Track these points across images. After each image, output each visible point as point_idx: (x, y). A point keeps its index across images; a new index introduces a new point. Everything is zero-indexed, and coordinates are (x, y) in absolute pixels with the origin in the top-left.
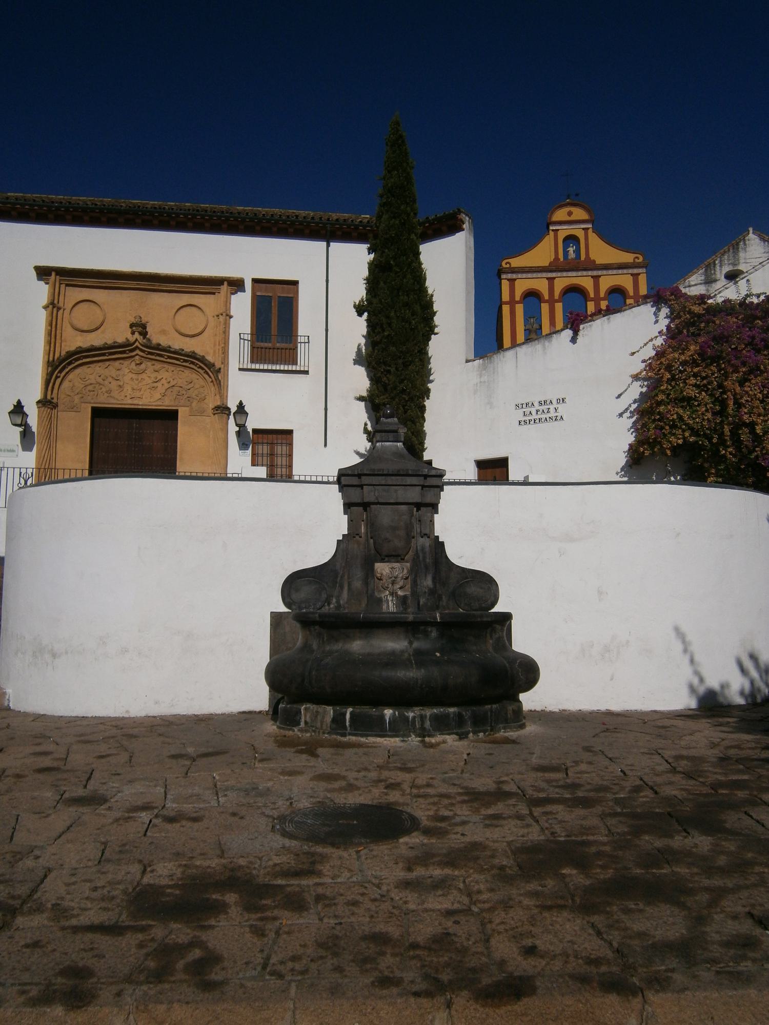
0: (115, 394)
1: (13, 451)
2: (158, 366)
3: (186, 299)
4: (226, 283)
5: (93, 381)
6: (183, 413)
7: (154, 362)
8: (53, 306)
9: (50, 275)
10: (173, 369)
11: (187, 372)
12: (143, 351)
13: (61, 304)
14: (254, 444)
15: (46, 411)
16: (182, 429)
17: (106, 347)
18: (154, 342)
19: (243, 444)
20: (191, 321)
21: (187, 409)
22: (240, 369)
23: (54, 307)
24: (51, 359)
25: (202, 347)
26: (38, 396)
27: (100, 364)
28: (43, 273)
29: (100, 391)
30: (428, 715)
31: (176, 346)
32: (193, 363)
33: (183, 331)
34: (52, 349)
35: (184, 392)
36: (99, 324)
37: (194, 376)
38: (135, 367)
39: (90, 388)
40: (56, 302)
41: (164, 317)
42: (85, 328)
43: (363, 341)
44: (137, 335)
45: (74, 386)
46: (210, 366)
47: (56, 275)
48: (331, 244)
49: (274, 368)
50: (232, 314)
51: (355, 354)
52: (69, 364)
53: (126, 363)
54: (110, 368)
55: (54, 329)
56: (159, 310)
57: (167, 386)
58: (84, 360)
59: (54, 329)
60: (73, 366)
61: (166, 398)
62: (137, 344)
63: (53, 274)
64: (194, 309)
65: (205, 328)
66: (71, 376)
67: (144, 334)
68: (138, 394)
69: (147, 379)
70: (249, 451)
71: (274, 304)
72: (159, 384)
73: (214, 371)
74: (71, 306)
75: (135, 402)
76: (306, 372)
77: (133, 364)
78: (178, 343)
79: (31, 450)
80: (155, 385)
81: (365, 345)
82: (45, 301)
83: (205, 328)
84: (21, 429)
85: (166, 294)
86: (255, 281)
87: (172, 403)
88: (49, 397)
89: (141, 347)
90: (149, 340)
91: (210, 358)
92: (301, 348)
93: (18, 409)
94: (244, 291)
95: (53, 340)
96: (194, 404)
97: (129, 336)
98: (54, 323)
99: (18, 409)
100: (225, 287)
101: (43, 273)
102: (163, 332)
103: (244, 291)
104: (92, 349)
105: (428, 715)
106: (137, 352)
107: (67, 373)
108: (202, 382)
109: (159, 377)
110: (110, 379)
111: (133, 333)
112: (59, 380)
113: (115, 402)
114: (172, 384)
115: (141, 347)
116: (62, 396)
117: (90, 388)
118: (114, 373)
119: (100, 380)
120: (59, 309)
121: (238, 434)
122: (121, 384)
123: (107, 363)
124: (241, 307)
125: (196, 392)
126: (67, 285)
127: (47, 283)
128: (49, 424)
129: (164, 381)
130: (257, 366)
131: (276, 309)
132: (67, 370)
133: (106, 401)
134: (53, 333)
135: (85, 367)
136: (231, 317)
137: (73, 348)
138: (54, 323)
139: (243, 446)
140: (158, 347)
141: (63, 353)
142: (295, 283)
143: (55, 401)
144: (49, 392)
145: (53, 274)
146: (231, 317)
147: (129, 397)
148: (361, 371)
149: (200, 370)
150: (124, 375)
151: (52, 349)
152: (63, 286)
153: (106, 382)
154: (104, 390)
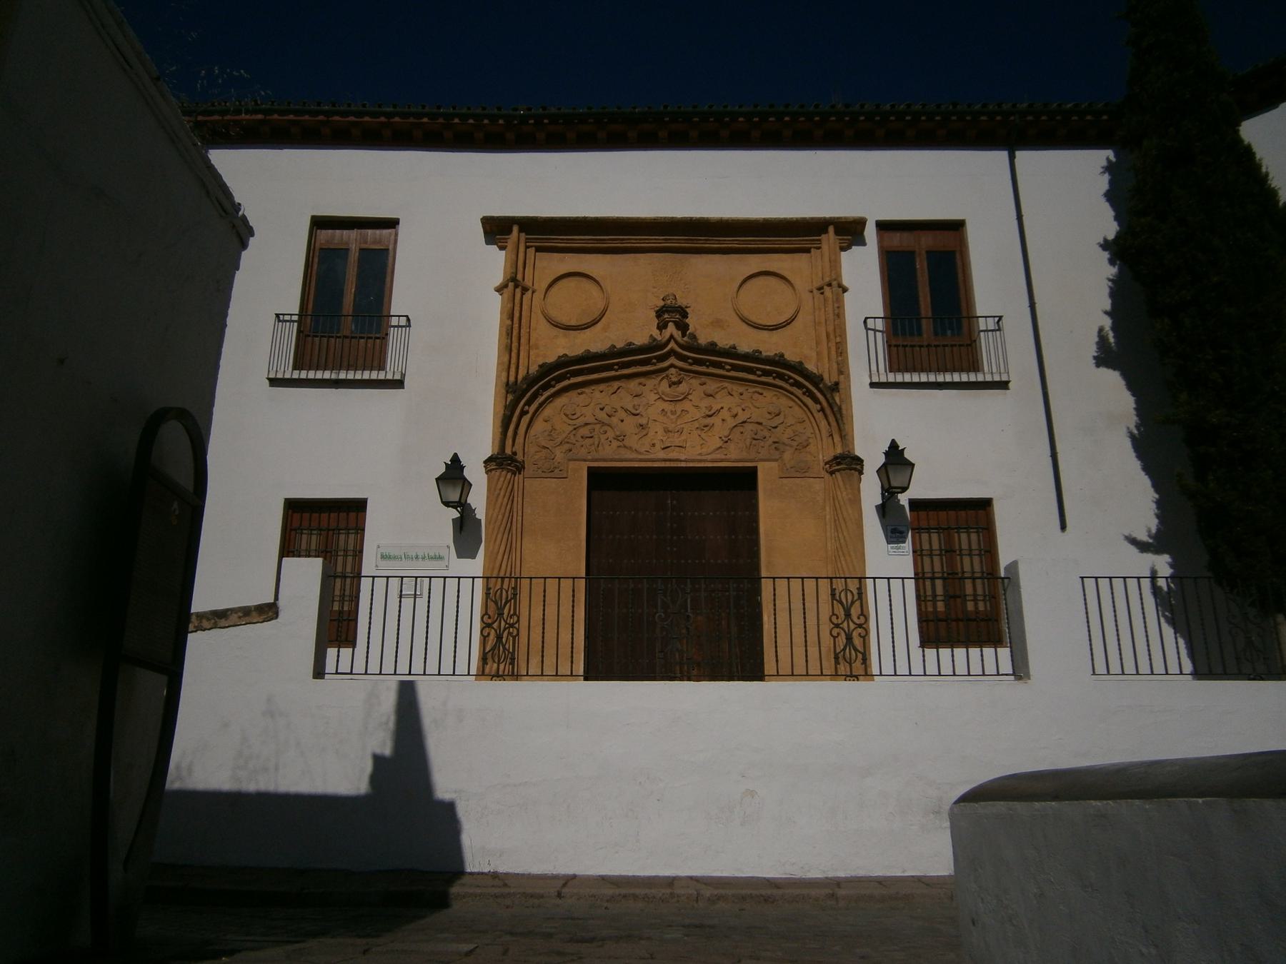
0: (632, 441)
1: (440, 558)
2: (712, 385)
3: (755, 263)
4: (831, 229)
5: (592, 420)
6: (766, 475)
7: (704, 379)
8: (514, 285)
9: (510, 232)
10: (741, 389)
11: (769, 394)
12: (683, 358)
13: (528, 282)
14: (917, 530)
15: (503, 476)
16: (767, 506)
17: (613, 353)
18: (703, 340)
19: (894, 531)
20: (769, 301)
21: (774, 464)
22: (873, 385)
23: (516, 286)
24: (512, 379)
25: (793, 345)
26: (487, 448)
27: (602, 386)
28: (496, 229)
29: (603, 437)
30: (354, 248)
31: (744, 348)
32: (781, 376)
33: (754, 318)
34: (514, 361)
35: (766, 433)
36: (596, 314)
37: (783, 402)
38: (668, 390)
39: (585, 431)
40: (519, 277)
41: (718, 297)
42: (573, 323)
43: (1107, 322)
44: (671, 328)
45: (553, 429)
46: (816, 380)
47: (520, 231)
48: (1018, 153)
49: (940, 379)
50: (845, 283)
51: (1094, 348)
52: (546, 387)
53: (651, 382)
54: (622, 393)
55: (516, 326)
56: (708, 286)
57: (731, 422)
58: (573, 380)
59: (516, 326)
60: (552, 390)
61: (732, 446)
62: (672, 345)
63: (515, 229)
64: (772, 281)
65: (797, 312)
66: (548, 411)
67: (683, 327)
68: (677, 440)
69: (692, 409)
70: (908, 546)
71: (921, 265)
72: (716, 420)
73: (823, 394)
74: (544, 285)
75: (673, 454)
76: (1003, 385)
77: (665, 383)
78: (747, 341)
79: (473, 556)
80: (708, 421)
81: (1113, 328)
82: (499, 279)
83: (797, 312)
84: (455, 514)
85: (717, 257)
86: (883, 226)
87: (745, 455)
88: (508, 451)
89: (679, 352)
90: (694, 337)
91: (811, 367)
92: (986, 344)
94: (864, 244)
95: (515, 345)
96: (787, 456)
97: (656, 333)
98: (517, 314)
100: (830, 239)
101: (496, 229)
102: (718, 323)
103: (864, 244)
104: (587, 357)
105: (354, 248)
106: (672, 360)
107: (541, 405)
108: (798, 412)
109: (716, 407)
110: (622, 414)
111: (662, 327)
112: (526, 419)
113: (634, 456)
114: (741, 418)
115: (679, 352)
116: (531, 449)
117: (585, 431)
118: (628, 402)
119: (602, 416)
120: (525, 290)
121: (882, 510)
122: (644, 421)
123: (616, 384)
124: (862, 272)
125: (789, 432)
126: (538, 249)
127: (502, 248)
128: (506, 501)
129: (725, 414)
130: (907, 378)
131: (927, 274)
132: (541, 399)
133: (612, 455)
134: (515, 333)
135: (573, 394)
136: (845, 290)
137: (551, 359)
138: (517, 314)
139: (894, 534)
140: (712, 349)
141: (534, 369)
142: (957, 227)
143: (519, 457)
144: (509, 442)
145: (515, 229)
146: (845, 290)
147: (658, 447)
148: (1112, 379)
149: (794, 389)
150: (648, 405)
151: (514, 361)
152: (531, 251)
153: (615, 420)
154: (611, 434)
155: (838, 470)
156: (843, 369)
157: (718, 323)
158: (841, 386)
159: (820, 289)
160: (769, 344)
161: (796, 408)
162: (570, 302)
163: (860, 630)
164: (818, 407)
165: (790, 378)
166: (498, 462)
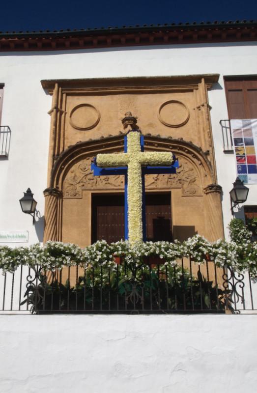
4: (203, 80)
6: (175, 195)
8: (58, 111)
9: (54, 87)
17: (103, 140)
20: (174, 114)
26: (45, 185)
28: (48, 86)
31: (164, 136)
32: (181, 149)
33: (168, 122)
36: (94, 122)
42: (84, 127)
46: (198, 150)
50: (210, 104)
56: (146, 107)
61: (159, 182)
66: (73, 168)
74: (70, 110)
82: (50, 108)
86: (227, 79)
87: (165, 186)
91: (196, 144)
93: (28, 197)
96: (185, 186)
99: (28, 197)
100: (202, 85)
101: (48, 86)
108: (190, 166)
111: (126, 127)
116: (66, 185)
125: (186, 175)
126: (68, 95)
137: (74, 143)
141: (66, 148)
155: (210, 192)
156: (212, 145)
157: (151, 125)
158: (211, 152)
159: (199, 108)
160: (176, 134)
161: (189, 163)
162: (82, 118)
163: (239, 284)
164: (200, 162)
165: (186, 149)
166: (49, 192)
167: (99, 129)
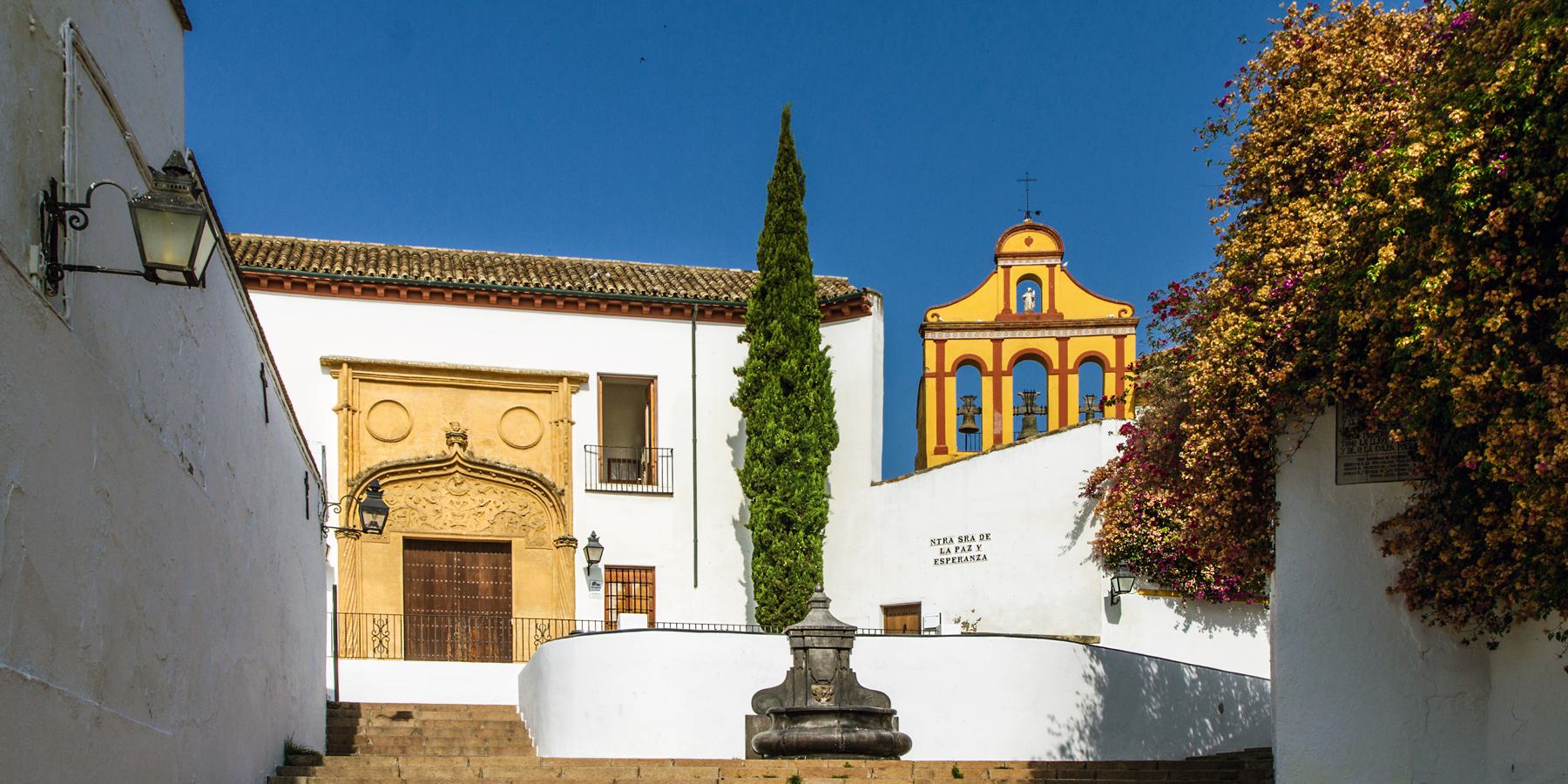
0: (431, 521)
2: (484, 486)
6: (517, 545)
8: (347, 408)
11: (521, 493)
13: (355, 407)
18: (478, 456)
20: (522, 429)
25: (536, 462)
37: (530, 499)
41: (490, 423)
50: (574, 419)
53: (443, 481)
56: (481, 414)
57: (496, 511)
67: (463, 446)
68: (460, 521)
72: (486, 509)
73: (551, 493)
77: (452, 485)
78: (508, 458)
90: (471, 454)
91: (547, 476)
96: (531, 534)
97: (445, 448)
102: (487, 442)
106: (457, 468)
108: (539, 506)
119: (411, 503)
123: (420, 482)
129: (491, 505)
133: (420, 530)
141: (364, 469)
153: (419, 506)
167: (411, 443)
